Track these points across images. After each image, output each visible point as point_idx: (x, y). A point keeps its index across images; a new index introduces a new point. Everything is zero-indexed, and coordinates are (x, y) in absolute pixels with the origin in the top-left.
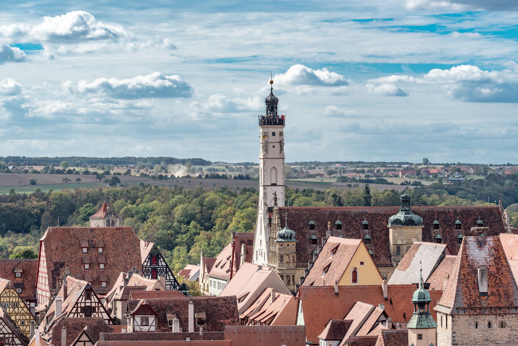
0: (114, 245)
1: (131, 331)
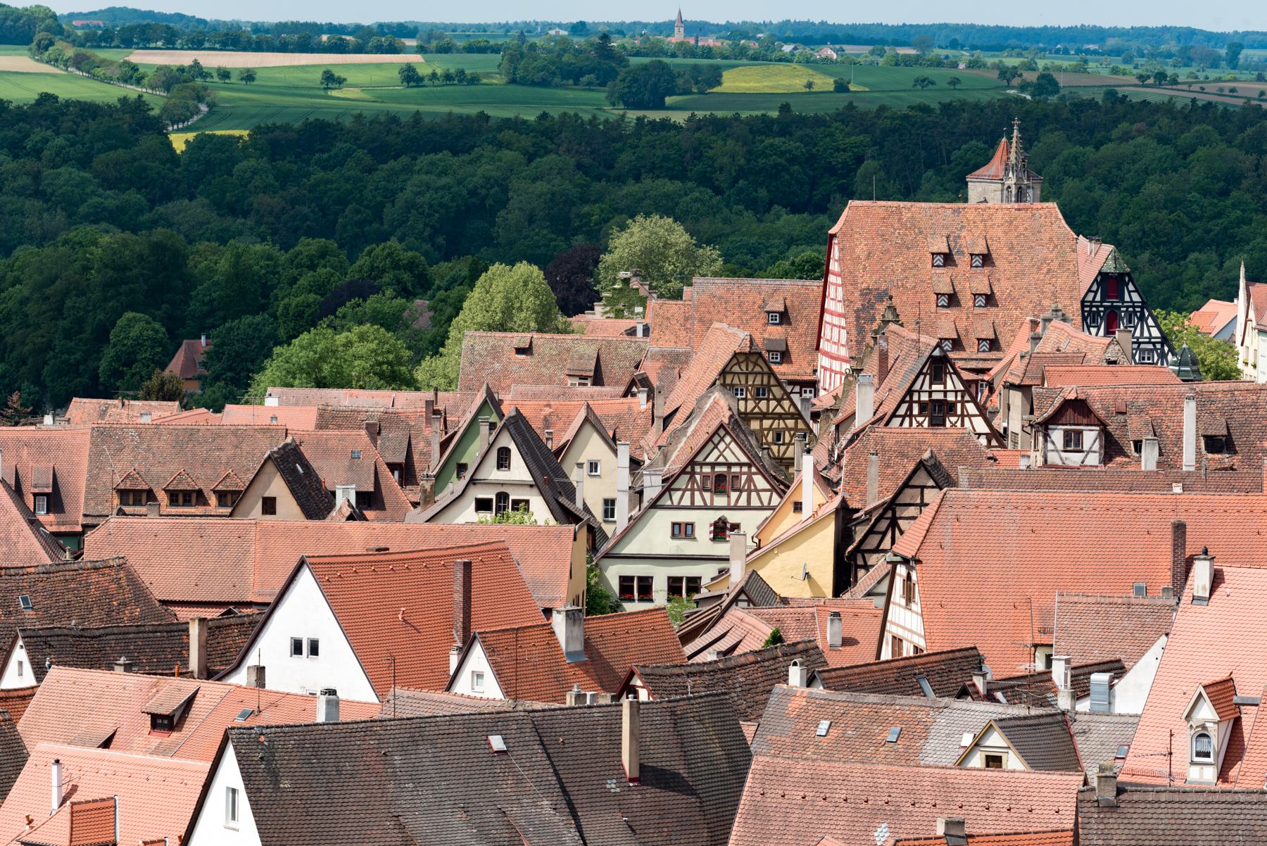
0: (1012, 248)
1: (1040, 462)
